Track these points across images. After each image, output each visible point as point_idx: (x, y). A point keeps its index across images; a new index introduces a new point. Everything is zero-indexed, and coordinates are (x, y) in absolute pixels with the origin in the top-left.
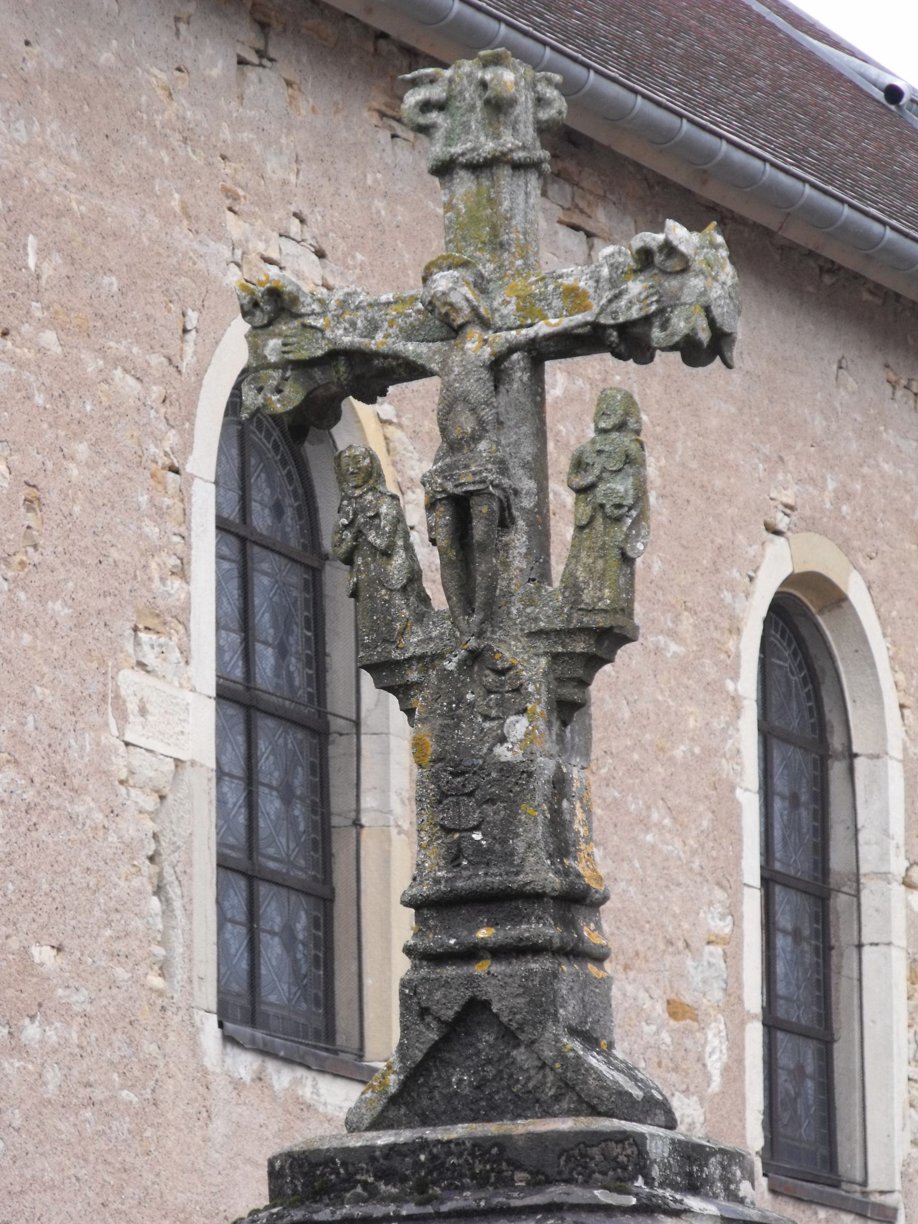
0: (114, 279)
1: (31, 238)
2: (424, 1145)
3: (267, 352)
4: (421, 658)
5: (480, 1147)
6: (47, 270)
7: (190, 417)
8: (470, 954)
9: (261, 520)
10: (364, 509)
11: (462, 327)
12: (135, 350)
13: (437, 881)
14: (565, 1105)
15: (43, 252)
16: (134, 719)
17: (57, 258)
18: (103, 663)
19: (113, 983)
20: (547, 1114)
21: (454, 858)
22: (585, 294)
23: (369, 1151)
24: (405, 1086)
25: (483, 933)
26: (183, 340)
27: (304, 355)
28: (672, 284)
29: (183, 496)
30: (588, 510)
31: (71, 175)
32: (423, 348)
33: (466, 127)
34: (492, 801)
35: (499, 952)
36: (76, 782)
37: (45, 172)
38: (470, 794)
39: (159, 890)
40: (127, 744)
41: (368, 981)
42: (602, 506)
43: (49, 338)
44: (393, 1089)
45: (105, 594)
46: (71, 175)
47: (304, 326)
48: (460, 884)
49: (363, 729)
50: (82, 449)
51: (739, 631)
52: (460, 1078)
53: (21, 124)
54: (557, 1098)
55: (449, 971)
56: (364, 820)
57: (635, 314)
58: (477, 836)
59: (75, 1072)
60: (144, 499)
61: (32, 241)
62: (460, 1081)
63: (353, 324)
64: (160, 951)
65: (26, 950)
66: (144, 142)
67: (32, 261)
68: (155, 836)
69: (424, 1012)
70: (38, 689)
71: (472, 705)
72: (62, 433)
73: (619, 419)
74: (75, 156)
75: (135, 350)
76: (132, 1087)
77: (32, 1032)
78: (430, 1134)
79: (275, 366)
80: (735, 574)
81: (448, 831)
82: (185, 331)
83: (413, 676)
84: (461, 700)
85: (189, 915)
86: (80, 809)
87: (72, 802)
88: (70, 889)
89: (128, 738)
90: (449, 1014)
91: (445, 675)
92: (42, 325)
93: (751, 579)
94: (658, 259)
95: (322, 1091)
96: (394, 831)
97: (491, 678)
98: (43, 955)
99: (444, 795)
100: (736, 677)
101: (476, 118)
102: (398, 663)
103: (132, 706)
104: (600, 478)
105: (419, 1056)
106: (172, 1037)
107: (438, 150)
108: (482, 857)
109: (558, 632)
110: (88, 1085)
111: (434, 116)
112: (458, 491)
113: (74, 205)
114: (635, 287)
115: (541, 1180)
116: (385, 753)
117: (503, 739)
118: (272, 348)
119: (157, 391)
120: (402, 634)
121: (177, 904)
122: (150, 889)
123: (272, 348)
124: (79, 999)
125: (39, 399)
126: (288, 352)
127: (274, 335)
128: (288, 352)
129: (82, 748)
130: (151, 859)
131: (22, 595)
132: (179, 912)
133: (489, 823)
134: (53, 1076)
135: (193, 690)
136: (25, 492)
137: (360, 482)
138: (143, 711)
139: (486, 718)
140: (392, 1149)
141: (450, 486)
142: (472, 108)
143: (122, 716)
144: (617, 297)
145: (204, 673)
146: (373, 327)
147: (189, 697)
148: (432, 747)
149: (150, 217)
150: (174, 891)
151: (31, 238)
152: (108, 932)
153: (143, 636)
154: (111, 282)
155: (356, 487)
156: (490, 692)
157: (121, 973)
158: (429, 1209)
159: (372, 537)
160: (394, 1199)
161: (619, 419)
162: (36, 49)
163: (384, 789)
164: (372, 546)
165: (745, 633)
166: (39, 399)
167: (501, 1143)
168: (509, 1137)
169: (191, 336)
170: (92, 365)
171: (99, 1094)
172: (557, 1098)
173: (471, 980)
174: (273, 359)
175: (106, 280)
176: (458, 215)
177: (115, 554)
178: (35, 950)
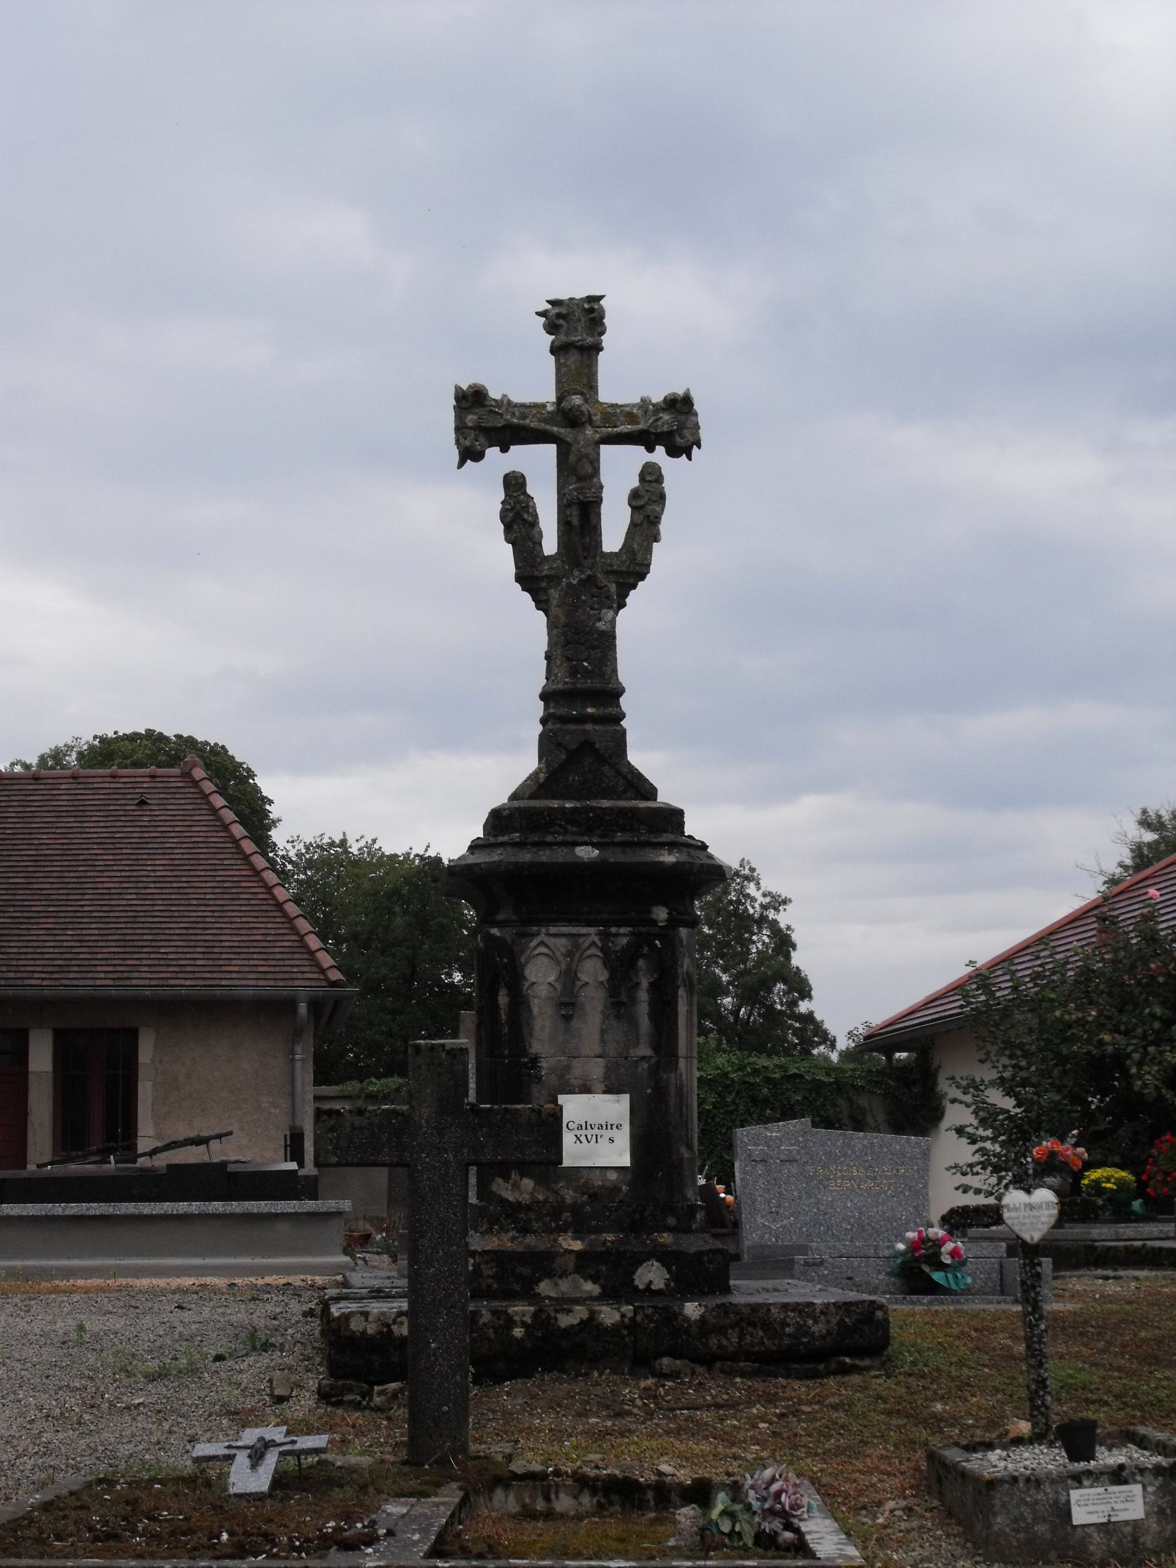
2: (593, 809)
3: (467, 420)
4: (547, 577)
5: (622, 811)
8: (583, 719)
10: (520, 502)
11: (583, 423)
13: (566, 683)
14: (628, 795)
20: (619, 798)
21: (573, 672)
22: (637, 416)
23: (562, 810)
24: (547, 779)
25: (589, 710)
27: (490, 425)
28: (683, 418)
30: (641, 517)
32: (562, 430)
33: (576, 329)
34: (594, 648)
35: (594, 719)
38: (583, 644)
42: (648, 517)
44: (542, 781)
47: (491, 411)
48: (579, 686)
52: (574, 778)
54: (624, 792)
55: (572, 727)
57: (665, 428)
62: (574, 780)
63: (513, 414)
69: (559, 745)
71: (584, 602)
73: (651, 477)
78: (593, 803)
79: (471, 428)
81: (569, 659)
83: (544, 585)
84: (579, 598)
91: (570, 585)
94: (679, 405)
97: (595, 590)
99: (569, 643)
101: (580, 326)
102: (537, 578)
104: (647, 503)
105: (557, 766)
108: (587, 673)
109: (622, 572)
111: (561, 321)
114: (666, 417)
115: (655, 829)
117: (600, 620)
118: (470, 419)
120: (540, 564)
123: (470, 419)
127: (471, 413)
139: (592, 608)
140: (574, 809)
141: (581, 497)
142: (579, 320)
144: (657, 420)
146: (524, 417)
148: (563, 619)
156: (593, 596)
158: (607, 840)
159: (526, 516)
160: (574, 833)
161: (651, 477)
164: (524, 520)
167: (635, 811)
168: (638, 808)
172: (624, 792)
173: (585, 732)
174: (470, 425)
176: (570, 370)
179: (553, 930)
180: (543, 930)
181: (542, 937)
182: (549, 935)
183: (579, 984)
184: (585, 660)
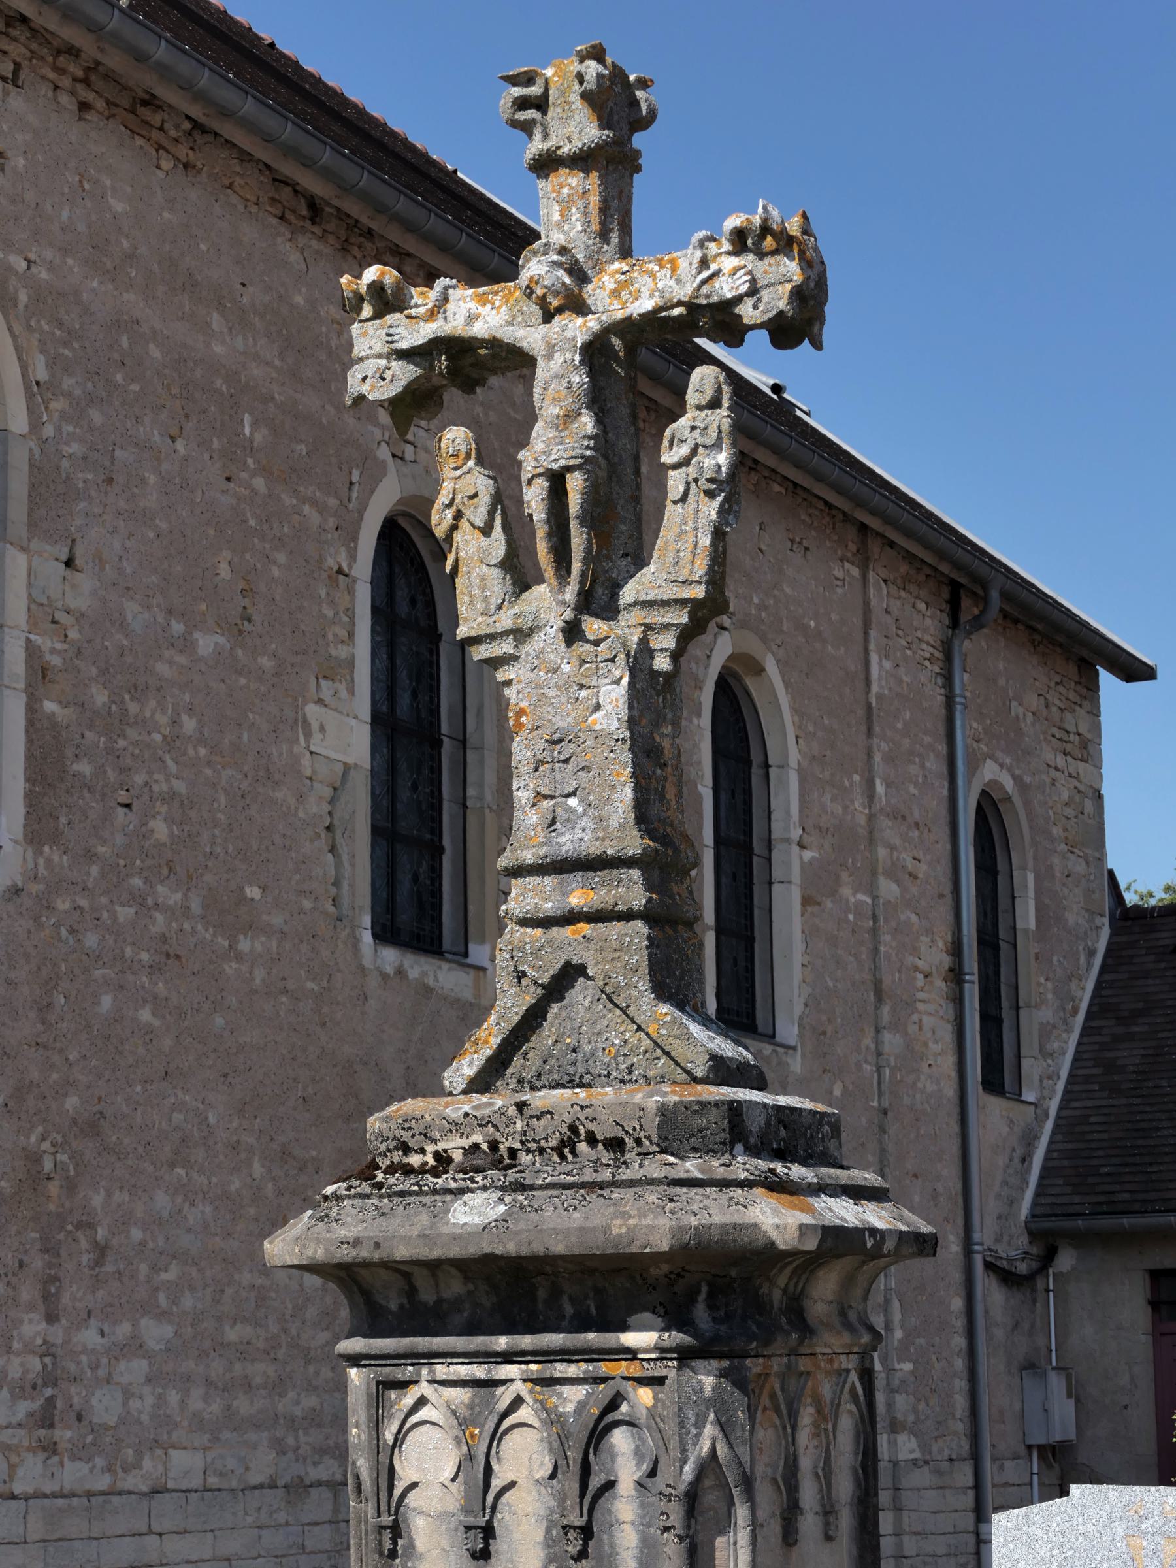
0: (303, 446)
1: (246, 415)
6: (258, 437)
7: (355, 538)
9: (403, 608)
12: (318, 494)
15: (255, 424)
16: (317, 737)
17: (265, 431)
18: (296, 700)
19: (301, 911)
26: (350, 489)
29: (351, 591)
31: (274, 375)
36: (277, 777)
37: (256, 371)
39: (333, 850)
40: (311, 753)
41: (471, 907)
43: (259, 483)
45: (297, 653)
46: (274, 375)
49: (468, 745)
50: (281, 558)
51: (701, 688)
53: (240, 338)
56: (468, 804)
58: (573, 802)
59: (274, 971)
60: (323, 593)
61: (247, 418)
64: (333, 890)
65: (242, 889)
66: (323, 357)
67: (247, 431)
68: (330, 813)
70: (251, 716)
72: (267, 546)
74: (277, 362)
75: (318, 494)
76: (314, 980)
77: (244, 945)
80: (699, 653)
82: (351, 483)
85: (353, 865)
86: (279, 795)
87: (273, 791)
88: (272, 848)
89: (312, 748)
90: (545, 979)
92: (254, 475)
93: (708, 657)
95: (440, 979)
96: (487, 811)
98: (253, 892)
100: (699, 715)
103: (315, 726)
106: (341, 945)
107: (536, 146)
110: (284, 979)
112: (555, 466)
113: (277, 396)
116: (481, 762)
119: (331, 522)
121: (345, 857)
122: (326, 849)
124: (277, 920)
125: (252, 523)
126: (392, 342)
128: (392, 342)
129: (280, 754)
130: (328, 828)
131: (240, 652)
132: (346, 865)
133: (584, 789)
134: (259, 974)
135: (356, 717)
136: (242, 584)
137: (460, 463)
138: (322, 729)
143: (308, 735)
145: (363, 704)
147: (353, 722)
149: (327, 407)
150: (344, 851)
151: (246, 415)
152: (297, 877)
153: (323, 683)
154: (302, 449)
155: (456, 469)
157: (307, 904)
162: (251, 289)
163: (481, 785)
165: (705, 689)
166: (252, 523)
169: (356, 487)
170: (288, 500)
171: (290, 985)
175: (299, 448)
177: (302, 627)
178: (248, 890)
179: (442, 1371)
180: (425, 1371)
181: (424, 1389)
182: (432, 1382)
183: (497, 1484)
184: (573, 794)
